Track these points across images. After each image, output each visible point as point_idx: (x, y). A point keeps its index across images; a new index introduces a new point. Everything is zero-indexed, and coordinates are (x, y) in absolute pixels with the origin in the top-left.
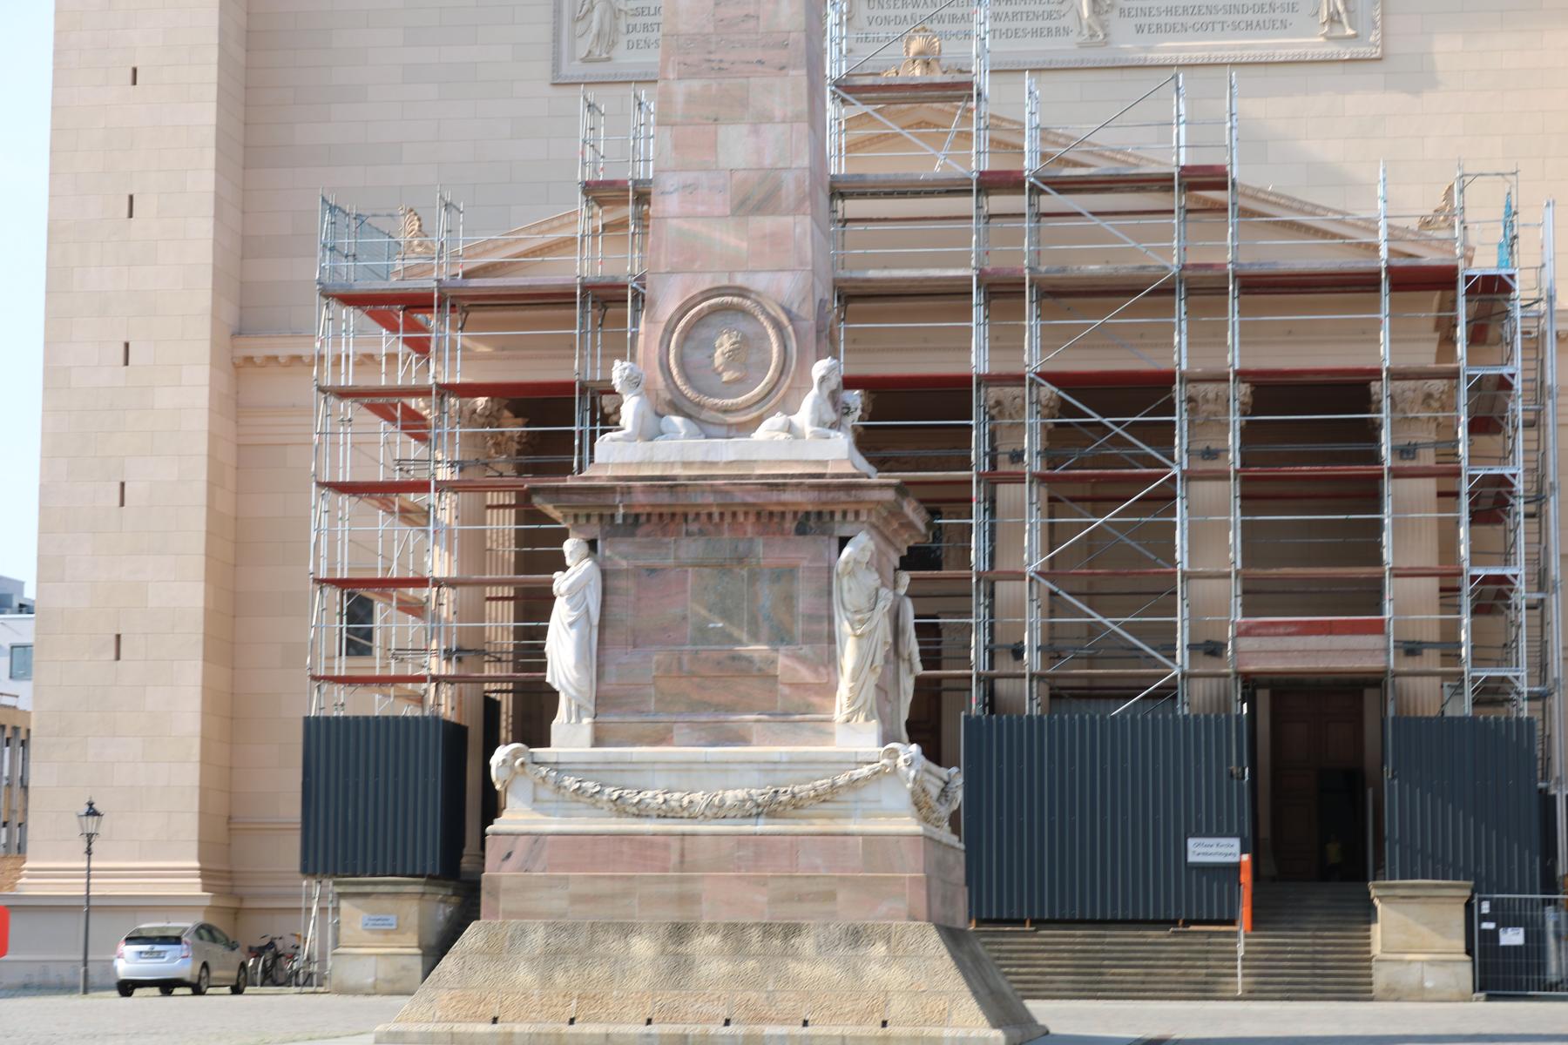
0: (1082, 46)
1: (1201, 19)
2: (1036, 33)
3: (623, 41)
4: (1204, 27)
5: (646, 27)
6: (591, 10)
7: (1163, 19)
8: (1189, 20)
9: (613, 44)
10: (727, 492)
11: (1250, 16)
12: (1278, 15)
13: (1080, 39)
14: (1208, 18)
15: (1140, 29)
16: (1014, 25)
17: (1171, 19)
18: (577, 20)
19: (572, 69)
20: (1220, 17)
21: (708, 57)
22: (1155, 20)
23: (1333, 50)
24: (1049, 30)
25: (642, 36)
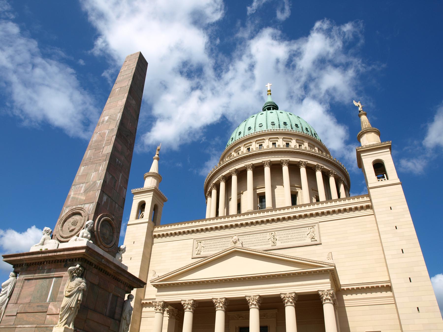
0: (272, 246)
1: (291, 240)
2: (265, 244)
3: (202, 251)
4: (292, 241)
5: (206, 249)
6: (198, 247)
7: (285, 241)
8: (289, 240)
9: (201, 251)
10: (54, 258)
11: (299, 239)
12: (304, 238)
13: (272, 245)
14: (293, 240)
15: (281, 243)
16: (261, 244)
17: (286, 241)
18: (196, 248)
19: (195, 256)
20: (294, 239)
21: (90, 161)
22: (284, 241)
23: (313, 243)
24: (267, 244)
25: (205, 250)
